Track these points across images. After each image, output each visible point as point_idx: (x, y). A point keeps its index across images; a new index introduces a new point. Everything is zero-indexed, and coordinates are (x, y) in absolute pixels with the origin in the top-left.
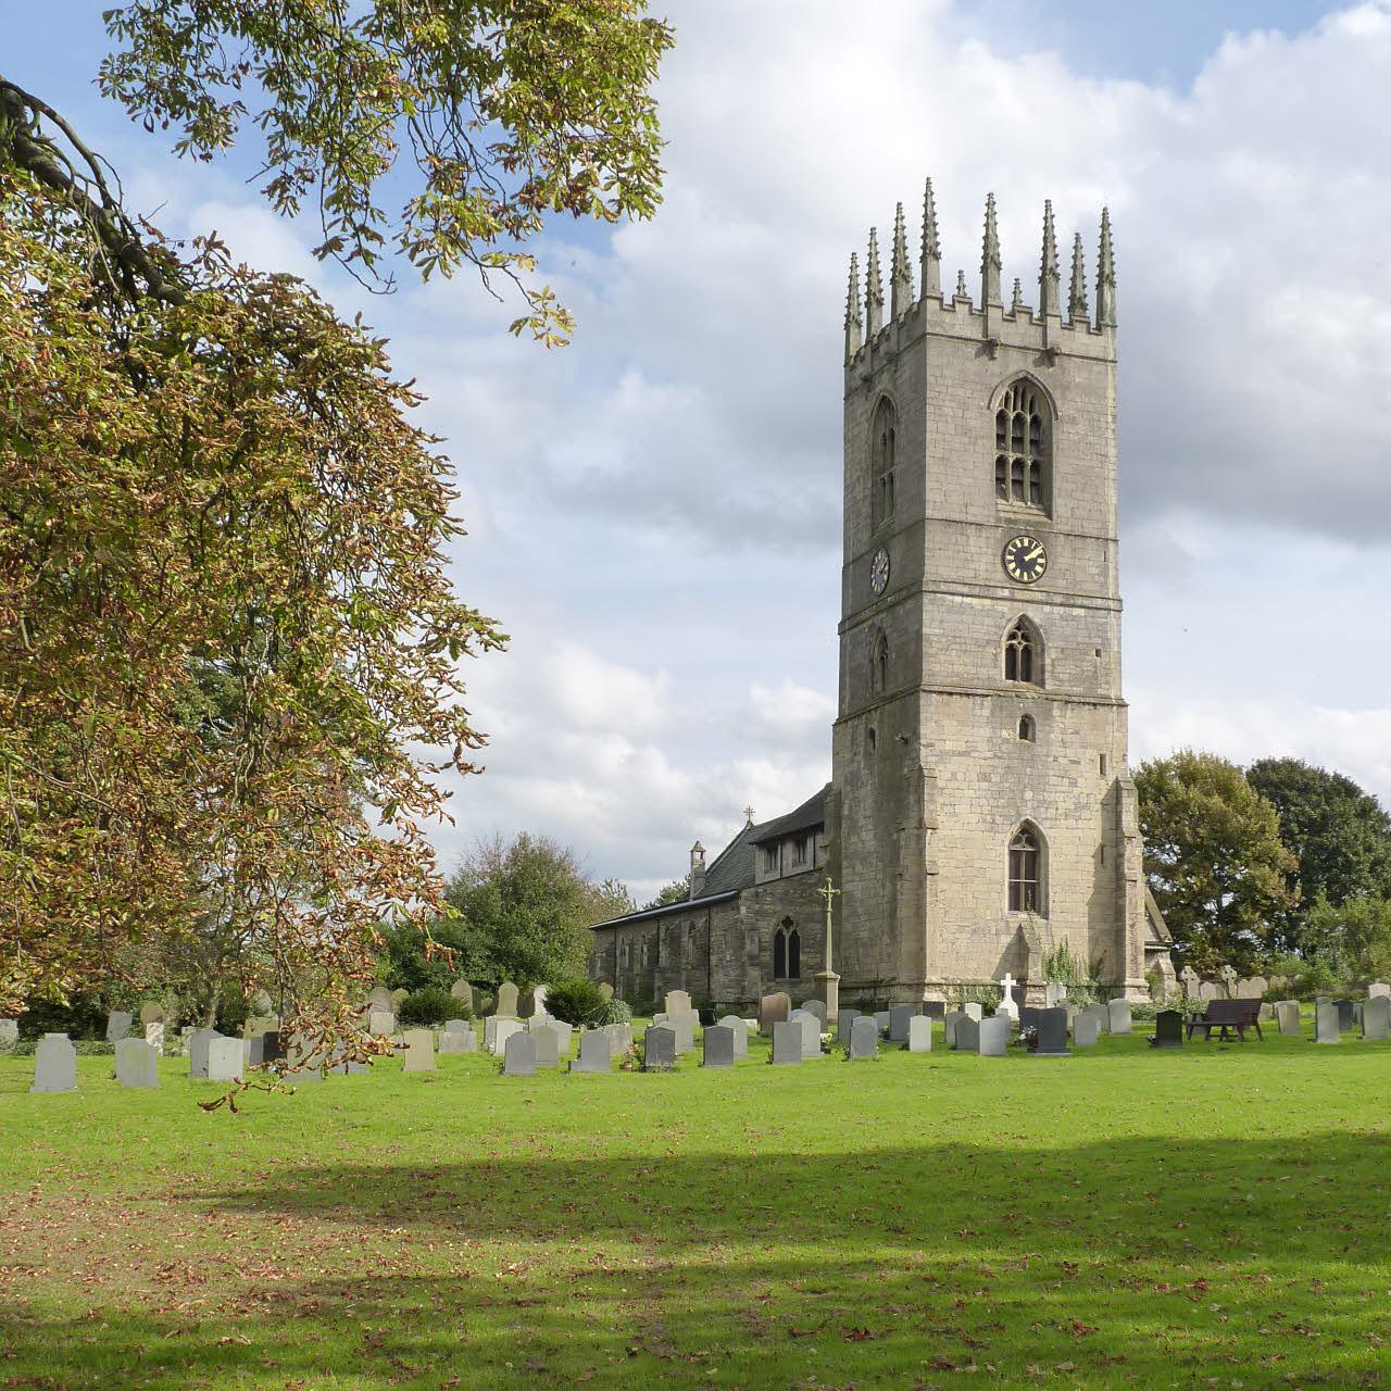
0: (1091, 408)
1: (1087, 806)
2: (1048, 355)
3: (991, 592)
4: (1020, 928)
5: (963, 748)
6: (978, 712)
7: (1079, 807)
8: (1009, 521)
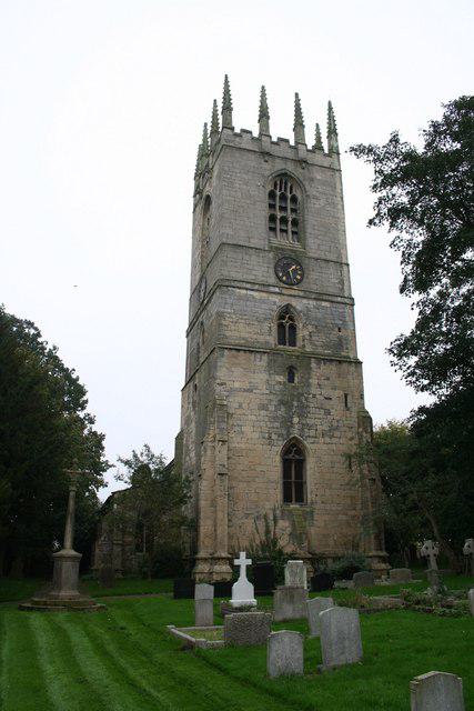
1: (337, 428)
5: (247, 386)
7: (331, 429)
8: (276, 248)
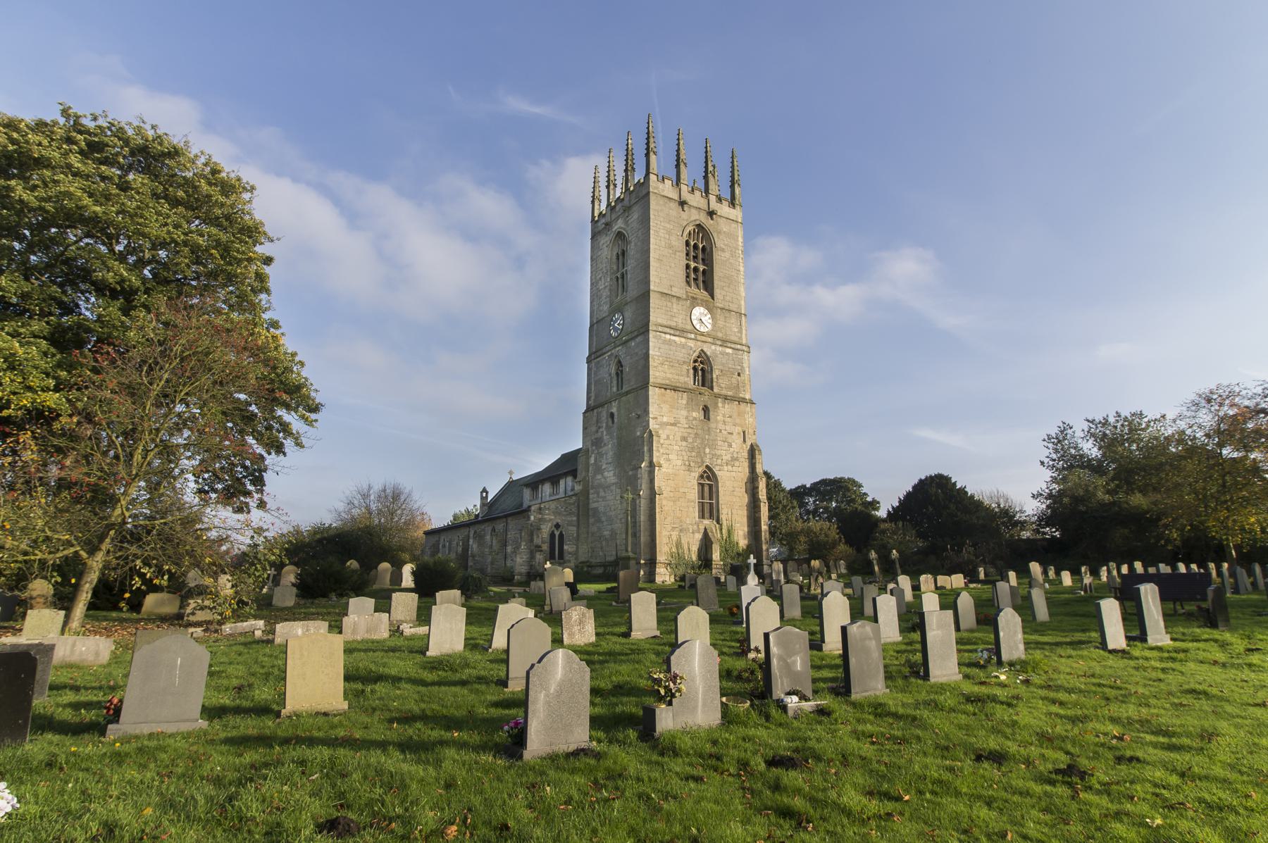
0: (731, 245)
1: (737, 459)
2: (711, 214)
3: (685, 335)
4: (705, 529)
6: (680, 401)
7: (734, 459)
